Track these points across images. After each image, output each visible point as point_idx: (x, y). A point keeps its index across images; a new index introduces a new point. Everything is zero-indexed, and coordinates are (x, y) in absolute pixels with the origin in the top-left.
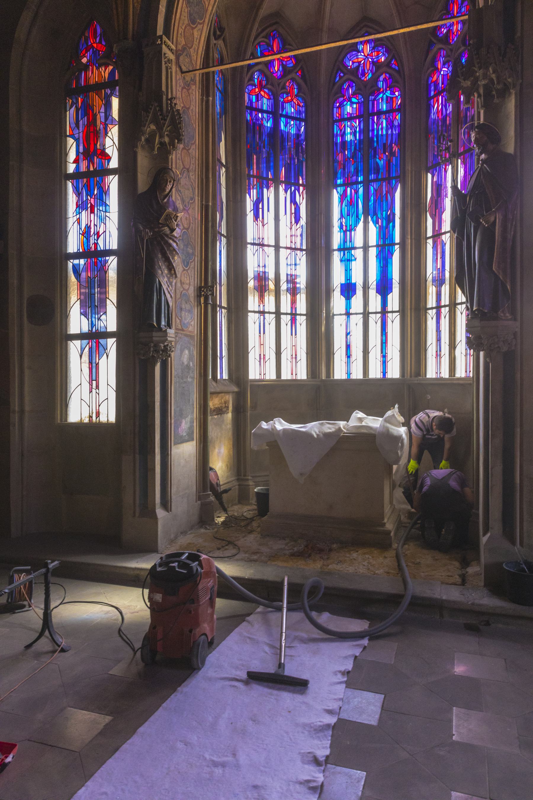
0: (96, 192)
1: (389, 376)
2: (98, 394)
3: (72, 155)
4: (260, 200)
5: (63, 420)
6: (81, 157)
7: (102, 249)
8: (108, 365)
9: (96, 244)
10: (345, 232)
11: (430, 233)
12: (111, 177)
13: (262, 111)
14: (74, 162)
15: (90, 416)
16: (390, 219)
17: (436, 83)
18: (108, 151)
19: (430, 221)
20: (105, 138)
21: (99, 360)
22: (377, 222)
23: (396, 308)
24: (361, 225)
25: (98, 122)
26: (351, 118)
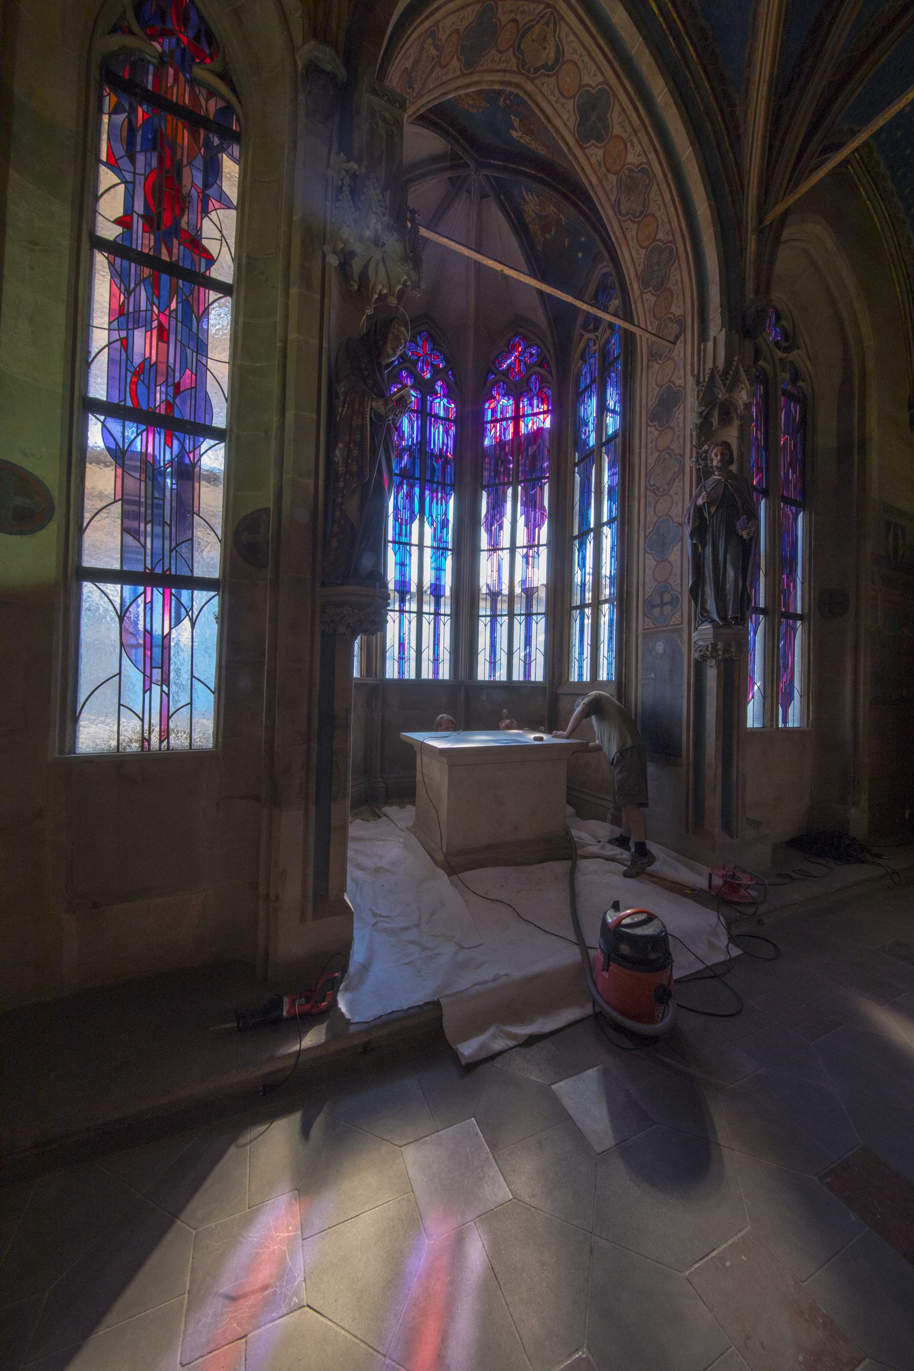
0: (173, 306)
1: (441, 677)
2: (168, 695)
5: (67, 750)
7: (187, 417)
10: (401, 525)
12: (213, 295)
14: (118, 222)
15: (143, 738)
16: (444, 524)
17: (494, 411)
18: (212, 247)
20: (202, 218)
21: (171, 629)
22: (432, 524)
23: (448, 611)
25: (186, 181)
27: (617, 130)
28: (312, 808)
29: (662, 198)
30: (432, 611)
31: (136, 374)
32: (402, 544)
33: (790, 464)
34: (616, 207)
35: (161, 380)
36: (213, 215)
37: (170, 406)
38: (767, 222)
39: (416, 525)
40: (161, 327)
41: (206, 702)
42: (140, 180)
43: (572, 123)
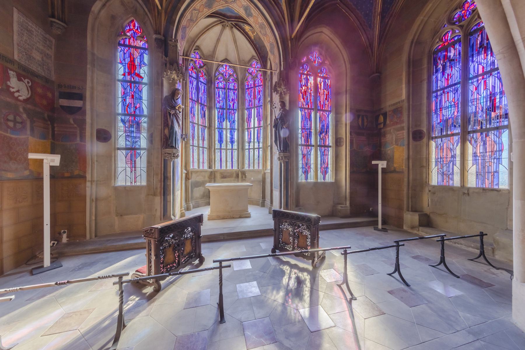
3: (121, 71)
4: (192, 108)
6: (127, 74)
8: (142, 162)
9: (135, 112)
11: (246, 127)
12: (143, 86)
13: (194, 78)
16: (234, 122)
17: (248, 85)
18: (142, 75)
19: (246, 124)
24: (225, 121)
26: (221, 88)
27: (254, 14)
28: (162, 197)
29: (268, 31)
30: (231, 148)
31: (127, 106)
32: (221, 129)
33: (326, 99)
34: (260, 32)
35: (133, 106)
36: (142, 68)
37: (135, 112)
38: (293, 37)
39: (224, 123)
40: (132, 95)
41: (144, 175)
42: (126, 65)
43: (244, 12)
